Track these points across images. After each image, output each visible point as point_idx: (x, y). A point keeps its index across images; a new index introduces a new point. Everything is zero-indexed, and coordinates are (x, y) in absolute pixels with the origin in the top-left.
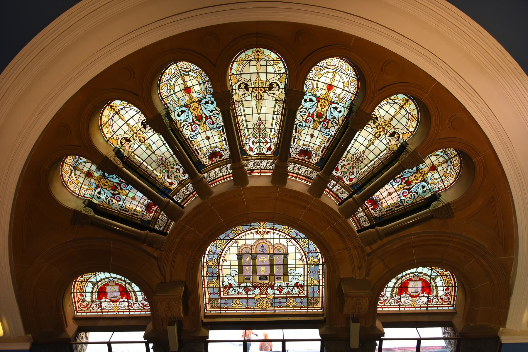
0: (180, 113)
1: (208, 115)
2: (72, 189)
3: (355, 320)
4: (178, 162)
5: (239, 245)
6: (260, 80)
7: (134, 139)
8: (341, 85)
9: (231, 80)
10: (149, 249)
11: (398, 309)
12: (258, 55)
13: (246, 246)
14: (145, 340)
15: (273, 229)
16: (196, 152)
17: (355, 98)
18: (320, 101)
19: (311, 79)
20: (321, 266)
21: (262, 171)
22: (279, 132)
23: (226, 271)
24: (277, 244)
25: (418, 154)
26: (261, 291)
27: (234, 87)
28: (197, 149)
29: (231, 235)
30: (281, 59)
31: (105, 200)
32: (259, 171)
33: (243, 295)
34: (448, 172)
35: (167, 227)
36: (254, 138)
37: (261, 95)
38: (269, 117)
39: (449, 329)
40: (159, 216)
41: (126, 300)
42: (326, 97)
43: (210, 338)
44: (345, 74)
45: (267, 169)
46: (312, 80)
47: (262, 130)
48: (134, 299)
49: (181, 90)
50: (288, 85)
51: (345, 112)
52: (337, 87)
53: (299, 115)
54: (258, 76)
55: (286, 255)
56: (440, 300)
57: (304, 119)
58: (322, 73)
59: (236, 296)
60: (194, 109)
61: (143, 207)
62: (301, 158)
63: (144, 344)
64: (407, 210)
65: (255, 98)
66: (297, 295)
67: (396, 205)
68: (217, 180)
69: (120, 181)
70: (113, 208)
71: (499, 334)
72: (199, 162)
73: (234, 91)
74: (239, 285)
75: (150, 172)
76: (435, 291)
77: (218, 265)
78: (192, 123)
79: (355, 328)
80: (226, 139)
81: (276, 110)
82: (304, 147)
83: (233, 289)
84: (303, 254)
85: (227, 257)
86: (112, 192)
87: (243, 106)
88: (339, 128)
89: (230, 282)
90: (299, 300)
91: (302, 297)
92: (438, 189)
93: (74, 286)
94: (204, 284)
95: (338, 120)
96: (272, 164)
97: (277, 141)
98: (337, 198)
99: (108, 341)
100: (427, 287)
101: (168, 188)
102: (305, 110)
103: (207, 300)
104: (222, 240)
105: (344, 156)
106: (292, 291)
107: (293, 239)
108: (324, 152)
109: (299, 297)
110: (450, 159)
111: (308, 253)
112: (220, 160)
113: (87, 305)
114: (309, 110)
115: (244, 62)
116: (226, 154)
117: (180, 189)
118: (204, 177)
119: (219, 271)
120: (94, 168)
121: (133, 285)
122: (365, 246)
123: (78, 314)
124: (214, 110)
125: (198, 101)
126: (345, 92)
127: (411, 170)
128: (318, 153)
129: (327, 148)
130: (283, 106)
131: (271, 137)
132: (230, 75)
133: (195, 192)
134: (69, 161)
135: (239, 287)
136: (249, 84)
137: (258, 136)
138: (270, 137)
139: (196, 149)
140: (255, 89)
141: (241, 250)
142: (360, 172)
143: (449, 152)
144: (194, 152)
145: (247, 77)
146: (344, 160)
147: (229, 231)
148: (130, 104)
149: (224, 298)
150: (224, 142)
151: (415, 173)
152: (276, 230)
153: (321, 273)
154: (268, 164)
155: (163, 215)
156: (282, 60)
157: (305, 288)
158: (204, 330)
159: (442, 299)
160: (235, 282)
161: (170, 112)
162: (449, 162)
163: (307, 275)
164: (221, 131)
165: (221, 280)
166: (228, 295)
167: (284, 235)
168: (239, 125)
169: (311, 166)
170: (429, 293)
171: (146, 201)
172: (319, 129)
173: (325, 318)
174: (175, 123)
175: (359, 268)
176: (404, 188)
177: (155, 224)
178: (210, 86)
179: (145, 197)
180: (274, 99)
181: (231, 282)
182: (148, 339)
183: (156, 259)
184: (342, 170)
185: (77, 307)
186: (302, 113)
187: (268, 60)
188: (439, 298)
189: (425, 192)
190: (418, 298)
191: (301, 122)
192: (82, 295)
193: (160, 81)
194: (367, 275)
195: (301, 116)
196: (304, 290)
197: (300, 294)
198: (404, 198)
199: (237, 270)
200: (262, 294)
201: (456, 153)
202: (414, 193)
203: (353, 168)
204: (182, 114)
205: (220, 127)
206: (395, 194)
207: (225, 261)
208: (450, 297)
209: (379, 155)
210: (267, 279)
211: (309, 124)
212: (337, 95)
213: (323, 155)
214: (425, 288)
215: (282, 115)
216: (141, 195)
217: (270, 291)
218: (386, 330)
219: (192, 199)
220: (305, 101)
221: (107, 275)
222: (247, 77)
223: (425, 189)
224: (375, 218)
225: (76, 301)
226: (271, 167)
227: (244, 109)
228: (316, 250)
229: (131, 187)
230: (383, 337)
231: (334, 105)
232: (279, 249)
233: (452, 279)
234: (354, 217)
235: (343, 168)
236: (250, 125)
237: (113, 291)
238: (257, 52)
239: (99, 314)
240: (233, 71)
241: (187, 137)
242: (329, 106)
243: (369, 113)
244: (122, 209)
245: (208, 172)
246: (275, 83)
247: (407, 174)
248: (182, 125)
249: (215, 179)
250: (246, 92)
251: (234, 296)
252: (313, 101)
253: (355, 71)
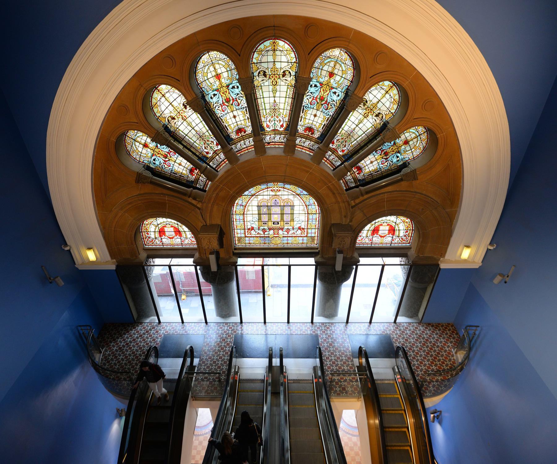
0: (213, 96)
1: (234, 98)
2: (134, 157)
3: (340, 252)
4: (212, 136)
5: (259, 200)
6: (275, 68)
7: (178, 118)
8: (340, 73)
9: (253, 68)
10: (194, 202)
11: (370, 245)
12: (274, 46)
13: (264, 200)
14: (194, 264)
15: (284, 188)
16: (225, 128)
17: (350, 84)
18: (322, 87)
19: (316, 68)
20: (318, 215)
21: (276, 143)
22: (290, 112)
23: (249, 218)
24: (286, 199)
25: (396, 131)
26: (274, 232)
27: (255, 74)
28: (227, 125)
29: (253, 192)
30: (293, 50)
31: (159, 165)
32: (274, 143)
33: (261, 234)
34: (417, 146)
35: (206, 186)
36: (270, 117)
37: (276, 81)
38: (283, 100)
39: (404, 259)
40: (199, 178)
41: (179, 237)
42: (328, 83)
43: (238, 263)
44: (343, 63)
45: (280, 142)
46: (317, 68)
47: (277, 110)
48: (185, 237)
49: (213, 77)
50: (298, 72)
51: (342, 96)
52: (337, 75)
53: (306, 98)
54: (274, 65)
55: (292, 207)
56: (401, 239)
57: (310, 102)
58: (325, 62)
59: (257, 236)
60: (223, 93)
61: (188, 171)
62: (306, 134)
63: (194, 267)
64: (383, 174)
65: (271, 83)
66: (300, 235)
67: (376, 171)
68: (242, 150)
69: (169, 150)
70: (165, 171)
71: (439, 263)
72: (228, 136)
73: (255, 77)
74: (259, 227)
75: (191, 144)
76: (397, 233)
77: (244, 214)
78: (222, 105)
79: (340, 258)
80: (249, 118)
81: (288, 94)
82: (309, 125)
83: (255, 231)
84: (305, 206)
85: (250, 208)
86: (164, 159)
87: (262, 91)
88: (336, 109)
89: (252, 225)
90: (301, 238)
91: (303, 237)
92: (408, 159)
93: (142, 227)
94: (234, 227)
95: (336, 103)
97: (288, 120)
98: (332, 165)
99: (168, 264)
100: (392, 230)
101: (205, 156)
102: (311, 94)
103: (236, 238)
104: (246, 195)
105: (339, 132)
106: (296, 232)
107: (298, 195)
108: (324, 129)
109: (301, 237)
110: (420, 135)
111: (309, 205)
112: (244, 134)
113: (152, 240)
114: (314, 94)
115: (263, 52)
116: (249, 130)
117: (215, 157)
118: (232, 148)
119: (244, 218)
120: (149, 140)
121: (184, 227)
122: (351, 201)
123: (146, 246)
124: (239, 94)
125: (226, 86)
126: (343, 79)
127: (389, 144)
128: (319, 129)
129: (327, 125)
130: (294, 90)
131: (284, 117)
132: (252, 64)
133: (226, 160)
134: (130, 135)
135: (259, 229)
136: (267, 71)
137: (274, 116)
138: (282, 117)
139: (225, 126)
140: (272, 76)
141: (260, 203)
142: (350, 145)
143: (420, 130)
144: (224, 128)
145: (265, 65)
146: (339, 135)
147: (252, 189)
148: (173, 88)
149: (248, 237)
150: (247, 120)
151: (392, 146)
152: (286, 189)
153: (318, 220)
154: (281, 138)
155: (203, 177)
156: (294, 51)
158: (234, 258)
159: (402, 239)
160: (255, 226)
161: (205, 95)
162: (419, 137)
163: (308, 221)
164: (245, 111)
165: (246, 224)
166: (251, 234)
167: (292, 192)
168: (258, 106)
169: (314, 140)
170: (393, 234)
171: (189, 165)
172: (321, 110)
173: (319, 251)
174: (209, 104)
175: (345, 217)
176: (382, 158)
177: (197, 183)
178: (236, 73)
179: (188, 163)
180: (287, 84)
181: (253, 226)
182: (196, 264)
183: (199, 209)
184: (337, 144)
185: (145, 242)
186: (308, 97)
187: (282, 51)
188: (400, 238)
189: (398, 161)
190: (385, 237)
191: (307, 104)
192: (148, 234)
193: (196, 69)
194: (351, 221)
195: (307, 99)
196: (304, 231)
197: (302, 234)
198: (382, 165)
199: (257, 217)
200: (275, 234)
201: (425, 131)
202: (390, 162)
203: (346, 142)
204: (214, 96)
205: (244, 108)
206: (376, 162)
207: (248, 210)
208: (408, 237)
209: (366, 131)
210: (278, 224)
211: (313, 106)
212: (337, 82)
213: (323, 131)
214: (391, 231)
215: (292, 98)
216: (186, 161)
217: (280, 232)
218: (360, 259)
219: (224, 165)
220: (311, 86)
221: (164, 219)
222: (265, 65)
223: (398, 159)
224: (359, 180)
225: (144, 237)
226: (283, 141)
227: (262, 93)
228: (314, 203)
229: (178, 155)
230: (358, 264)
231: (334, 90)
232: (288, 203)
233: (411, 225)
234: (344, 180)
235: (338, 142)
236: (267, 106)
237: (169, 231)
238: (273, 43)
239: (161, 246)
240: (254, 61)
241: (219, 116)
242: (330, 91)
243: (361, 97)
244: (172, 172)
245: (235, 144)
246: (287, 71)
247: (387, 146)
248: (214, 106)
249: (241, 150)
250: (265, 78)
251: (255, 236)
252: (317, 87)
253: (352, 61)
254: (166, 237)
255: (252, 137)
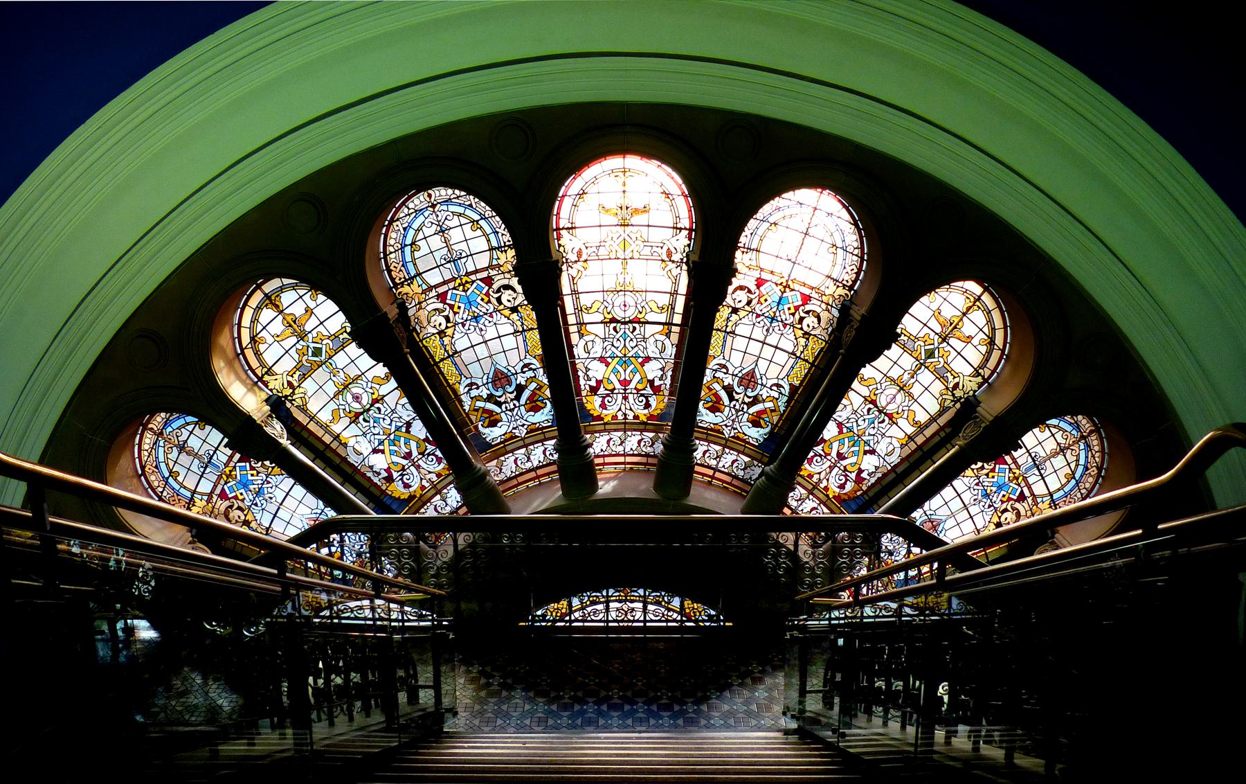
68: (521, 479)
96: (653, 444)
255: (552, 438)
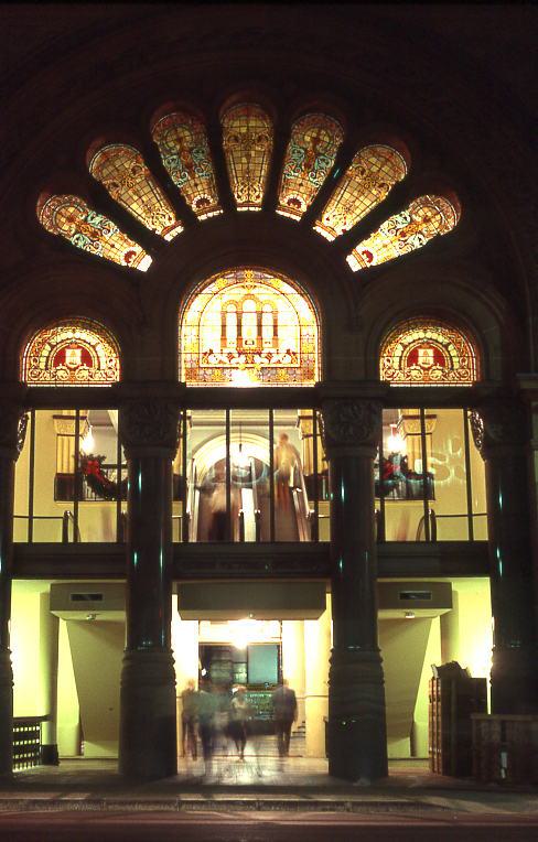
157: (298, 356)
192: (35, 361)
217: (257, 357)
254: (64, 368)
